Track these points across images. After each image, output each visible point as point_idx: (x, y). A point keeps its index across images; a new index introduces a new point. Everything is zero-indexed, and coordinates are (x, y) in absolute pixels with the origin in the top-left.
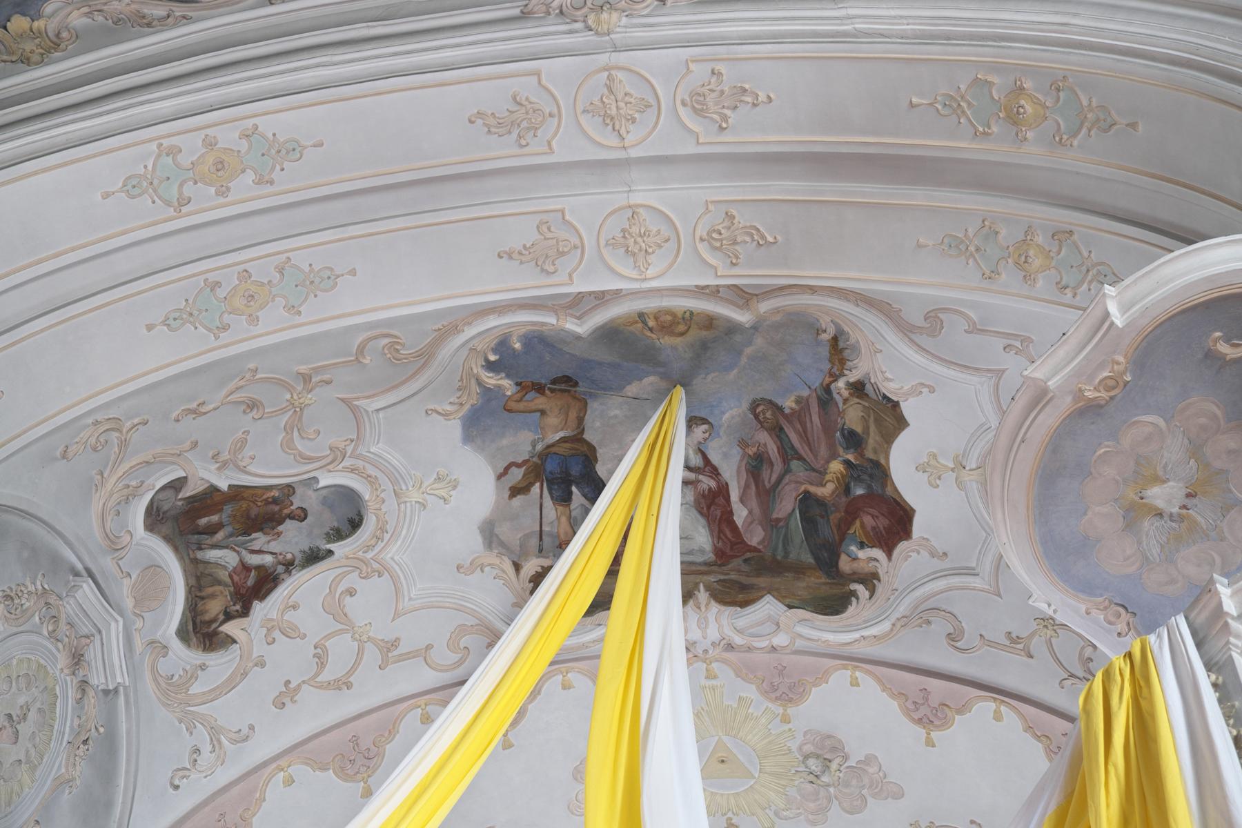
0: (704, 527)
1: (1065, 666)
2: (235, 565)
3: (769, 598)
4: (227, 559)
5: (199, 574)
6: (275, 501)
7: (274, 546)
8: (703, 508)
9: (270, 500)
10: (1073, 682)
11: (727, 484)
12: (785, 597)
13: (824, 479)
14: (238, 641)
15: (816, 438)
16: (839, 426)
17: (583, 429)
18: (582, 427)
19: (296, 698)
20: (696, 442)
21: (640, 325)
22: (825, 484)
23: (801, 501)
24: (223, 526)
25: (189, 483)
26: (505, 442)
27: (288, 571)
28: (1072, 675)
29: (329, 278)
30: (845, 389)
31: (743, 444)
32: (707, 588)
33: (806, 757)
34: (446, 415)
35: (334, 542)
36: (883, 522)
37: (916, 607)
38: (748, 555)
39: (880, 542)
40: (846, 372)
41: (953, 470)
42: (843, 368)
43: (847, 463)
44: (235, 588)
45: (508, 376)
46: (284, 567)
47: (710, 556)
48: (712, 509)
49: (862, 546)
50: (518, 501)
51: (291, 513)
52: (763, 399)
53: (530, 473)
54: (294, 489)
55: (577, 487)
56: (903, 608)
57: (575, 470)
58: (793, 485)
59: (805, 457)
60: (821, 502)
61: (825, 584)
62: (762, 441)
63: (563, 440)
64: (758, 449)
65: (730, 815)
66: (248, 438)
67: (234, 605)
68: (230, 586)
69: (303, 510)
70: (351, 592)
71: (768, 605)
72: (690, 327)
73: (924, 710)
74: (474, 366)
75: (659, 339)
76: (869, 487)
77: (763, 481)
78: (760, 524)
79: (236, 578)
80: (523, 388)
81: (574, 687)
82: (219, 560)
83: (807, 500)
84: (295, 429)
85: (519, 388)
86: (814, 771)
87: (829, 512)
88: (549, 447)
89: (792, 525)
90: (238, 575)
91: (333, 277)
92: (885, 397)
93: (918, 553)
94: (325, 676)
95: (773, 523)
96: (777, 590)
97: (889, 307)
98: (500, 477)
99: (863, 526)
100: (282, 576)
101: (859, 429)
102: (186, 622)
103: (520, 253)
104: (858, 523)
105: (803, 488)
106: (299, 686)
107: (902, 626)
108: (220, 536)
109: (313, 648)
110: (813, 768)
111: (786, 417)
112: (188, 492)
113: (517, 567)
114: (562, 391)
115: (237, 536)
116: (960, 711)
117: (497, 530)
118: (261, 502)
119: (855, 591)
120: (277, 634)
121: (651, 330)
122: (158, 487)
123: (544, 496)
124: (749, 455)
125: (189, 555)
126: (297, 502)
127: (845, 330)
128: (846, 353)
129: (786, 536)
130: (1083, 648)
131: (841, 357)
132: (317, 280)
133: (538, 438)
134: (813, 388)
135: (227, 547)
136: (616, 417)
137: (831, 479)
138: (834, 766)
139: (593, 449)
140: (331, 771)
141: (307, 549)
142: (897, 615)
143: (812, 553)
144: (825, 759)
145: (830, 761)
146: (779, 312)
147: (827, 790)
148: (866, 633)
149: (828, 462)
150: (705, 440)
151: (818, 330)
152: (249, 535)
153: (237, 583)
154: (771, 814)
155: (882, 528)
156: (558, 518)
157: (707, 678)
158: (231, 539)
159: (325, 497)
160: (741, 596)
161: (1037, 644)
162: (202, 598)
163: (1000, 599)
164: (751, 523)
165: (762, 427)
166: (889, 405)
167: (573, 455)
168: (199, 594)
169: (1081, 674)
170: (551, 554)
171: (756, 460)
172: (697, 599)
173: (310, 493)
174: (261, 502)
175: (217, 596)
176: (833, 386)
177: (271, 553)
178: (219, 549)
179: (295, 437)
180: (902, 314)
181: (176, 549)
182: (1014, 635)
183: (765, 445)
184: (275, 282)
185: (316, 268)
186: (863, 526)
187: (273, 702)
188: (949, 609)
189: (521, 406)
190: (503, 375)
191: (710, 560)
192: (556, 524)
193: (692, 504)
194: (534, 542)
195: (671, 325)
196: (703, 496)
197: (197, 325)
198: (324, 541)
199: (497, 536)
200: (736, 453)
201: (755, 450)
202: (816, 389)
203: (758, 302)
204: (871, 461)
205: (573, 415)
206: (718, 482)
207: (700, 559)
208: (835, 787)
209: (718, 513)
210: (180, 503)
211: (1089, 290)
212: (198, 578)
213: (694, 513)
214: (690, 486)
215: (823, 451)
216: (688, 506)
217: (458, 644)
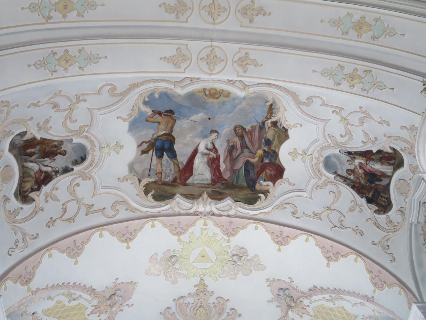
0: (209, 171)
1: (333, 223)
3: (229, 198)
4: (35, 167)
6: (55, 146)
7: (52, 164)
8: (210, 164)
9: (54, 146)
10: (336, 228)
11: (220, 156)
12: (235, 197)
13: (255, 156)
14: (35, 200)
15: (255, 141)
16: (264, 137)
17: (172, 131)
18: (172, 130)
19: (54, 224)
20: (211, 139)
21: (203, 93)
22: (255, 158)
23: (245, 163)
24: (35, 154)
26: (143, 133)
27: (56, 175)
28: (336, 226)
29: (97, 58)
30: (270, 124)
31: (228, 141)
32: (207, 193)
33: (233, 255)
34: (124, 120)
35: (75, 165)
36: (273, 173)
37: (281, 202)
38: (224, 182)
39: (271, 180)
40: (272, 117)
41: (302, 155)
42: (271, 116)
43: (264, 151)
45: (150, 108)
47: (210, 182)
48: (213, 164)
49: (265, 180)
50: (144, 155)
51: (61, 152)
52: (239, 125)
53: (150, 146)
55: (166, 153)
56: (277, 203)
57: (166, 146)
58: (243, 158)
59: (249, 147)
60: (252, 164)
61: (249, 193)
62: (235, 141)
63: (164, 134)
64: (233, 144)
65: (202, 276)
66: (51, 119)
67: (35, 186)
68: (34, 178)
69: (65, 151)
70: (78, 185)
71: (229, 200)
72: (220, 96)
73: (280, 239)
74: (139, 102)
75: (208, 99)
76: (270, 160)
77: (233, 155)
78: (229, 171)
79: (37, 175)
80: (154, 113)
81: (156, 227)
82: (32, 167)
83: (247, 163)
84: (69, 118)
85: (153, 113)
86: (236, 260)
87: (255, 168)
88: (158, 136)
89: (241, 171)
90: (38, 174)
91: (98, 58)
92: (284, 127)
93: (285, 183)
94: (66, 216)
95: (234, 171)
96: (232, 195)
97: (295, 94)
98: (139, 146)
99: (266, 173)
100: (54, 177)
101: (271, 138)
102: (17, 190)
103: (168, 59)
104: (264, 173)
105: (246, 159)
106: (56, 219)
107: (276, 209)
108: (33, 157)
109: (62, 206)
110: (236, 259)
111: (246, 133)
112: (26, 138)
113: (140, 181)
114: (168, 115)
115: (40, 159)
116: (293, 239)
117: (134, 167)
118: (50, 146)
119: (260, 196)
120: (49, 199)
121: (206, 95)
122: (16, 134)
123: (153, 155)
124: (230, 146)
125: (21, 164)
126: (63, 148)
127: (276, 102)
128: (274, 111)
129: (238, 176)
130: (340, 217)
131: (272, 112)
132: (92, 59)
133: (155, 133)
134: (259, 122)
136: (185, 127)
137: (257, 156)
138: (243, 258)
139: (174, 139)
140: (65, 253)
142: (274, 205)
143: (246, 182)
144: (240, 256)
145: (241, 257)
146: (254, 93)
147: (238, 267)
148: (262, 211)
149: (257, 150)
150: (215, 139)
151: (266, 101)
152: (44, 159)
154: (217, 276)
155: (273, 175)
156: (157, 164)
157: (204, 225)
158: (37, 159)
160: (219, 196)
161: (323, 216)
162: (24, 182)
163: (312, 200)
164: (226, 170)
165: (237, 136)
166: (284, 131)
167: (167, 141)
168: (23, 180)
169: (339, 225)
170: (153, 177)
171: (232, 147)
172: (203, 197)
174: (50, 146)
175: (29, 181)
176: (266, 123)
177: (51, 167)
178: (33, 163)
180: (299, 98)
181: (17, 161)
182: (316, 213)
183: (236, 142)
184: (77, 56)
185: (93, 53)
186: (266, 173)
188: (293, 204)
189: (152, 120)
190: (149, 107)
191: (209, 183)
192: (156, 166)
193: (206, 162)
194: (147, 172)
195: (214, 94)
196: (211, 159)
197: (46, 68)
198: (71, 165)
199: (134, 168)
200: (225, 145)
201: (232, 144)
202: (259, 123)
203: (249, 88)
204: (273, 150)
205: (170, 125)
206: (217, 155)
207: (206, 182)
208: (241, 266)
209: (215, 166)
210: (22, 142)
211: (374, 91)
213: (206, 166)
214: (206, 156)
215: (257, 146)
216: (204, 163)
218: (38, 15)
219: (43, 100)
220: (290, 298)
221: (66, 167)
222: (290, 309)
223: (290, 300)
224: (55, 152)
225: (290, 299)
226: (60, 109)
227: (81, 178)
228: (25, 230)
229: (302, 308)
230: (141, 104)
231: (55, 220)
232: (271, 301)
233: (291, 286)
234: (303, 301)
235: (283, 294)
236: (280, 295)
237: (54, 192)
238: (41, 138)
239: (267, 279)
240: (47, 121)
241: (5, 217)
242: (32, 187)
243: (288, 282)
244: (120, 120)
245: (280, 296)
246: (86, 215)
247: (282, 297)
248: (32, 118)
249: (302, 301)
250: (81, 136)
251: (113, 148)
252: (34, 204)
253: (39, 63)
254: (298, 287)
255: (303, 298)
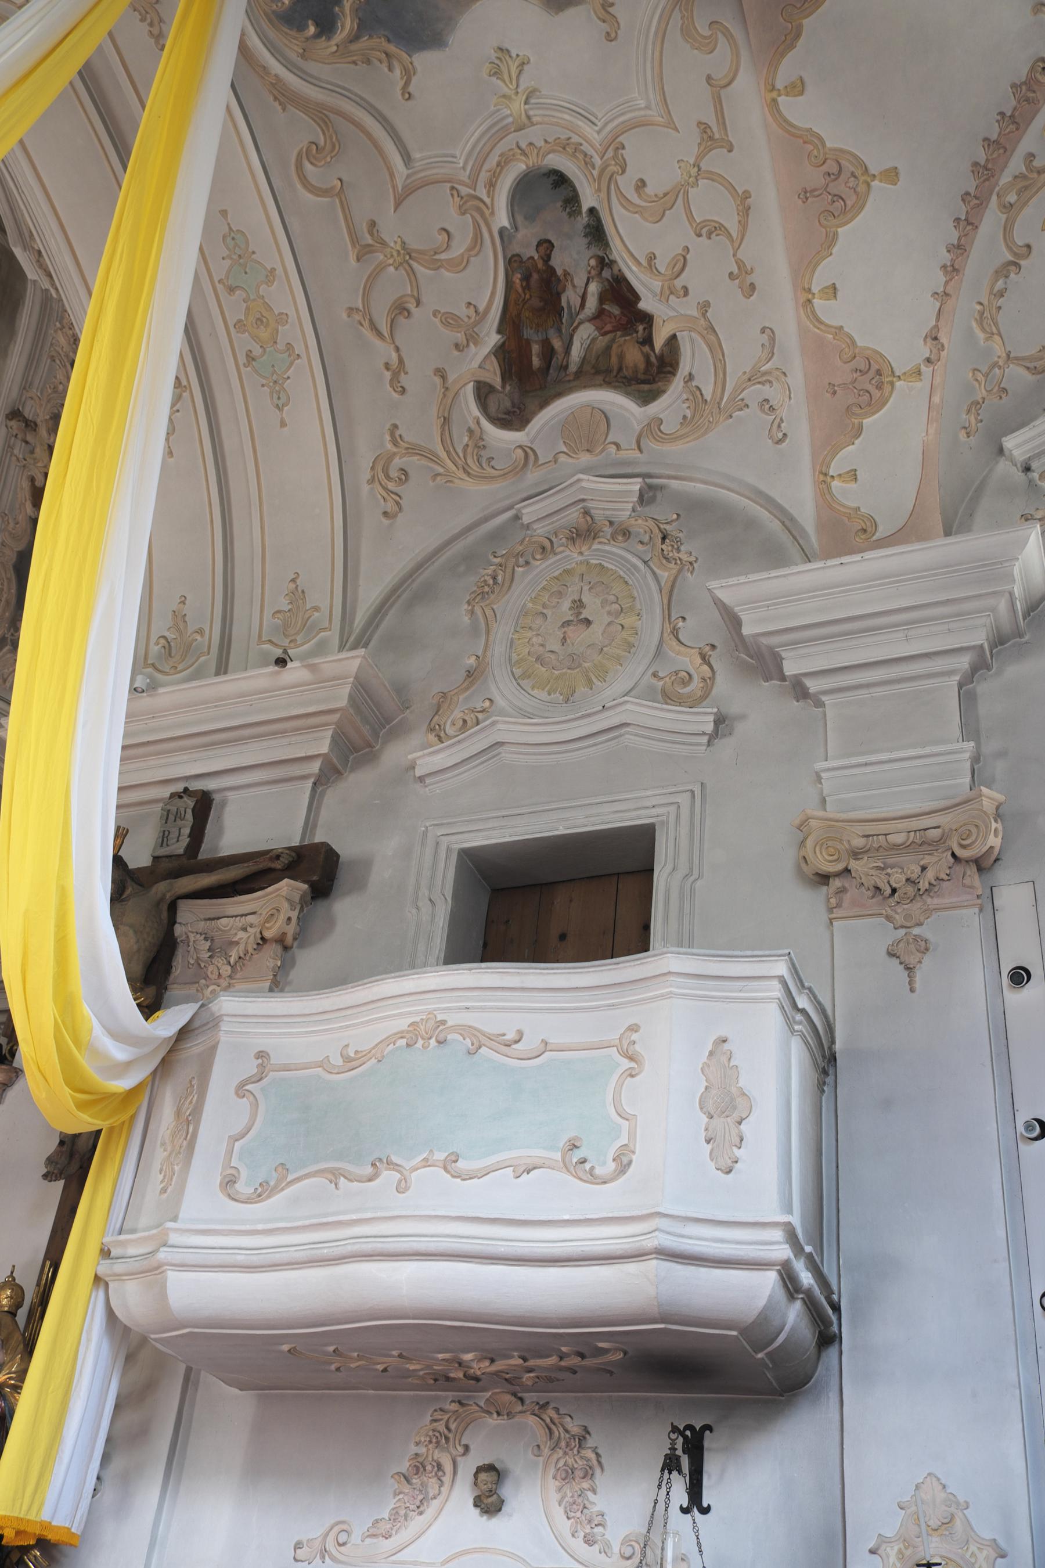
2: (594, 328)
4: (585, 337)
5: (593, 371)
6: (527, 278)
7: (580, 280)
9: (524, 284)
14: (671, 333)
24: (547, 339)
25: (482, 379)
27: (612, 263)
29: (233, 239)
34: (409, 74)
35: (580, 206)
44: (619, 330)
46: (605, 268)
51: (542, 258)
54: (513, 256)
66: (442, 311)
67: (637, 332)
68: (615, 335)
69: (539, 244)
70: (641, 184)
79: (608, 327)
84: (437, 257)
90: (606, 325)
91: (232, 234)
94: (733, 226)
100: (616, 271)
102: (639, 391)
103: (151, 24)
108: (557, 344)
109: (701, 238)
115: (562, 323)
120: (679, 283)
125: (569, 381)
126: (530, 252)
132: (238, 251)
135: (571, 337)
140: (839, 230)
141: (586, 241)
152: (563, 308)
153: (613, 327)
158: (564, 331)
159: (526, 218)
162: (620, 369)
168: (615, 374)
173: (519, 235)
179: (446, 257)
181: (559, 395)
184: (244, 295)
185: (226, 253)
187: (746, 297)
190: (337, 9)
197: (285, 376)
210: (508, 388)
212: (598, 372)
217: (705, 38)
218: (177, 414)
219: (385, 351)
221: (586, 236)
224: (545, 276)
226: (409, 293)
227: (619, 178)
228: (745, 372)
230: (333, 42)
231: (740, 264)
237: (661, 265)
238: (499, 331)
240: (449, 320)
241: (688, 442)
242: (638, 342)
244: (411, 89)
246: (730, 151)
248: (441, 373)
250: (488, 201)
251: (511, 83)
252: (683, 338)
253: (275, 396)
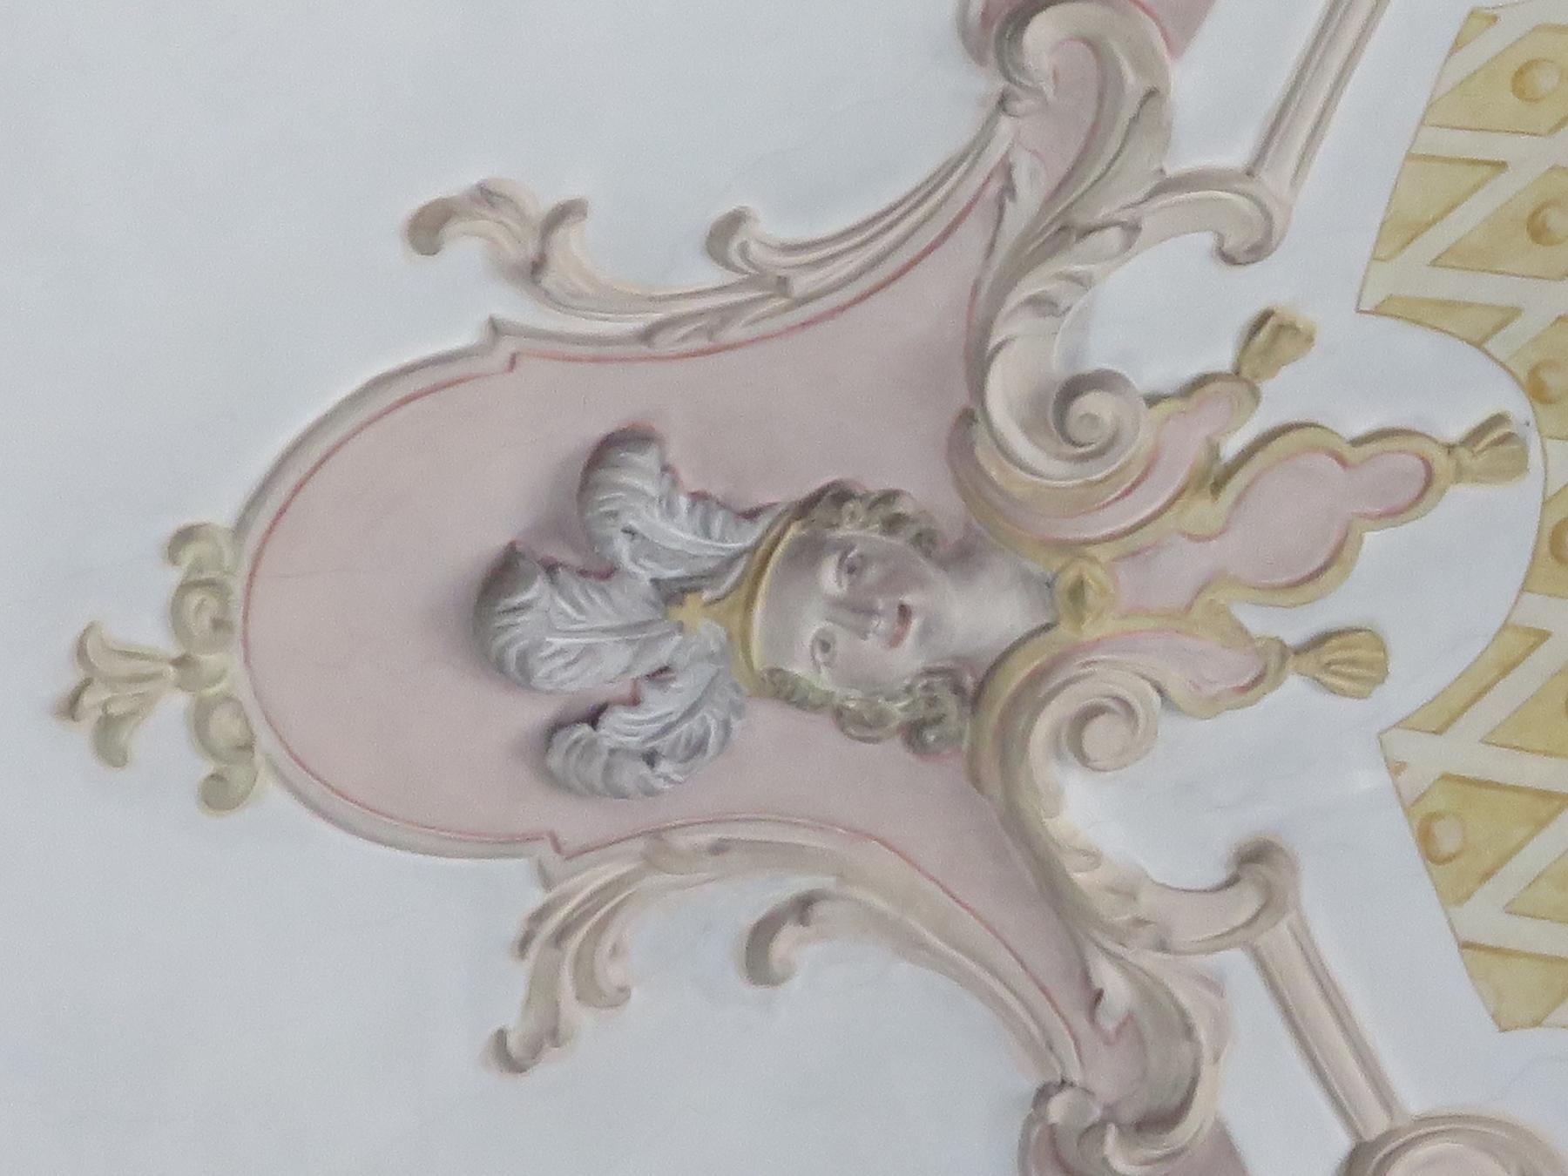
220: (808, 553)
222: (1010, 744)
223: (857, 609)
225: (830, 578)
229: (1204, 512)
232: (542, 988)
233: (599, 351)
234: (1095, 362)
235: (628, 630)
236: (593, 718)
239: (70, 707)
243: (496, 329)
245: (619, 728)
247: (661, 704)
249: (1074, 388)
254: (735, 221)
255: (1042, 305)
